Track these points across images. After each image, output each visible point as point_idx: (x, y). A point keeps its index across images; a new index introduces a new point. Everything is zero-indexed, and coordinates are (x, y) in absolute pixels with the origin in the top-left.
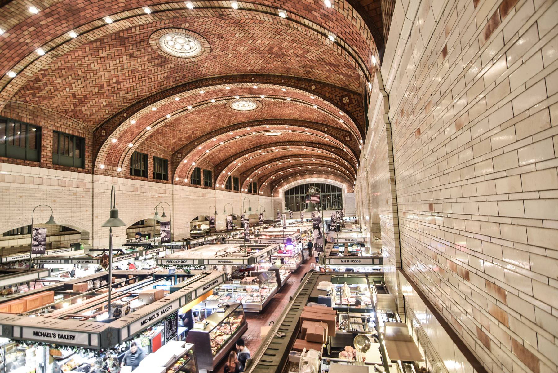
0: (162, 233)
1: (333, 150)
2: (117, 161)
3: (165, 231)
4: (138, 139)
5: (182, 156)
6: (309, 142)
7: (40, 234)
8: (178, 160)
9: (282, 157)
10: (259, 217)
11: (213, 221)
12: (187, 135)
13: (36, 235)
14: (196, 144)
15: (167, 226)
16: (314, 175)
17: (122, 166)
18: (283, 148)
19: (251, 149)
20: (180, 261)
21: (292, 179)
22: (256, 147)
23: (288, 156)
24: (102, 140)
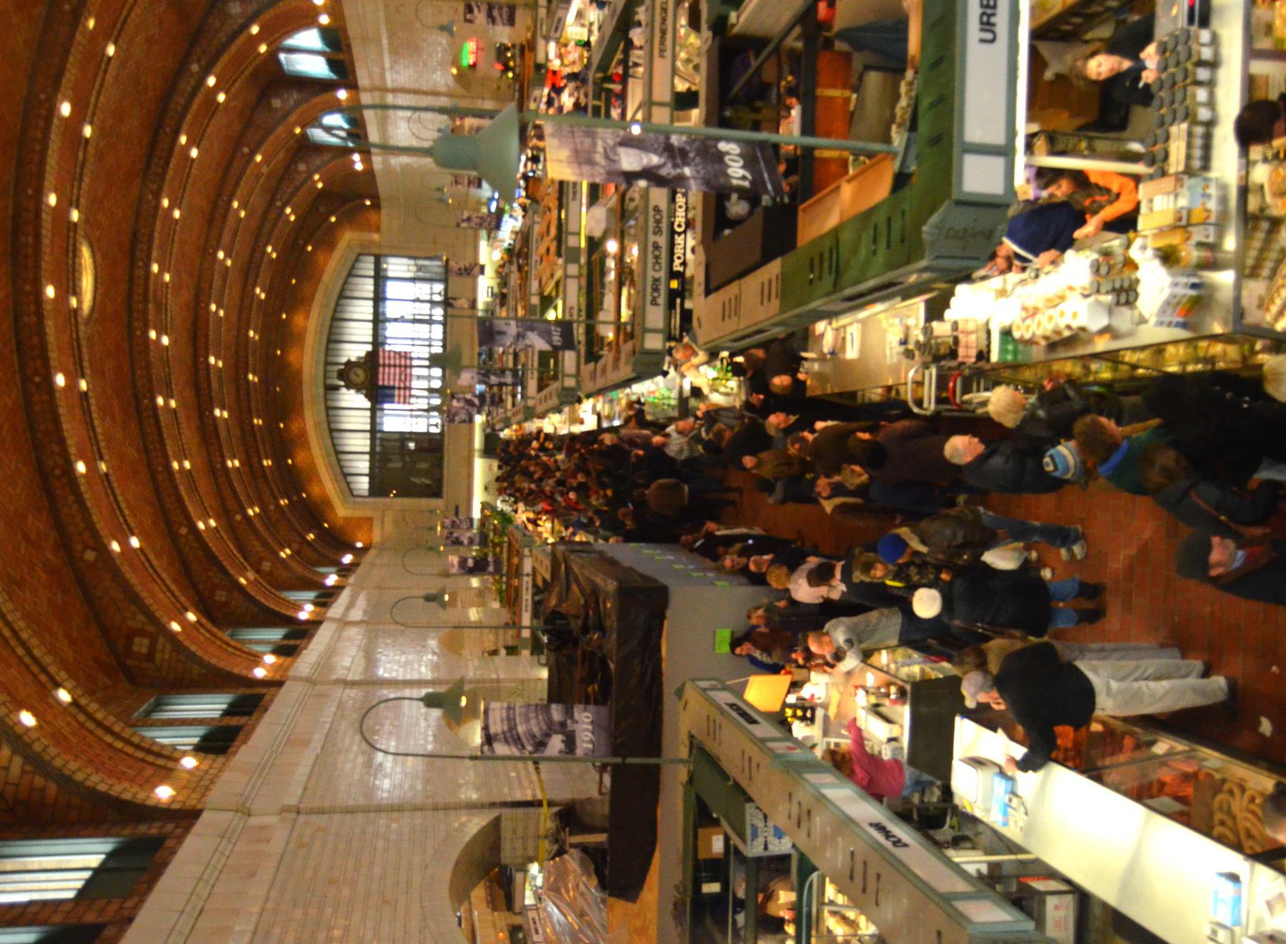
0: (528, 342)
1: (195, 68)
2: (141, 764)
3: (520, 336)
4: (36, 660)
5: (142, 633)
6: (148, 167)
7: (512, 728)
8: (164, 653)
9: (197, 387)
10: (462, 404)
11: (470, 563)
12: (44, 576)
13: (517, 741)
14: (90, 556)
15: (497, 328)
16: (292, 357)
17: (169, 758)
18: (161, 307)
19: (143, 436)
20: (652, 238)
21: (301, 457)
22: (138, 410)
23: (195, 357)
24: (18, 761)
